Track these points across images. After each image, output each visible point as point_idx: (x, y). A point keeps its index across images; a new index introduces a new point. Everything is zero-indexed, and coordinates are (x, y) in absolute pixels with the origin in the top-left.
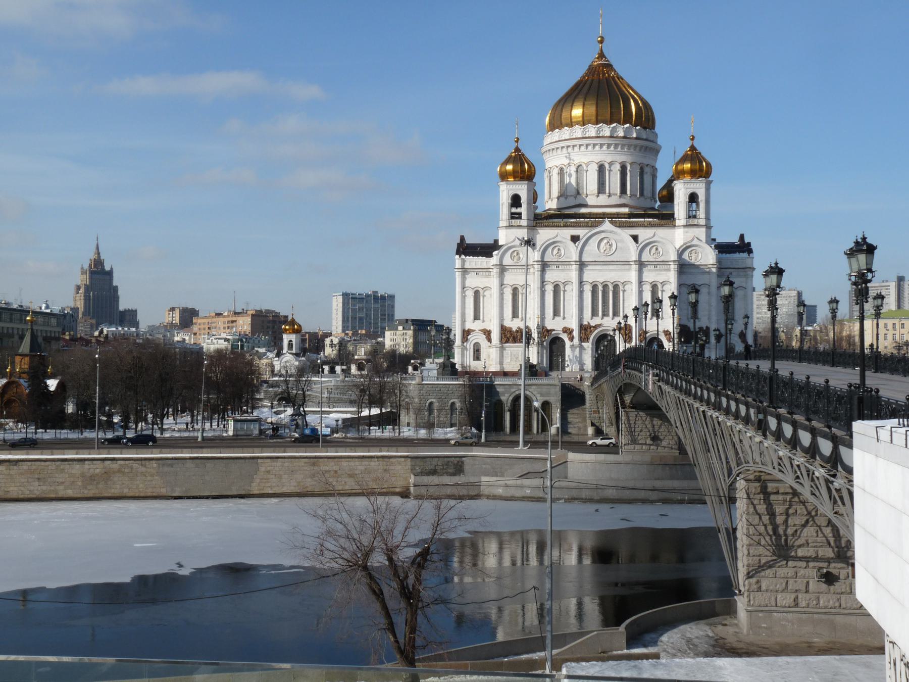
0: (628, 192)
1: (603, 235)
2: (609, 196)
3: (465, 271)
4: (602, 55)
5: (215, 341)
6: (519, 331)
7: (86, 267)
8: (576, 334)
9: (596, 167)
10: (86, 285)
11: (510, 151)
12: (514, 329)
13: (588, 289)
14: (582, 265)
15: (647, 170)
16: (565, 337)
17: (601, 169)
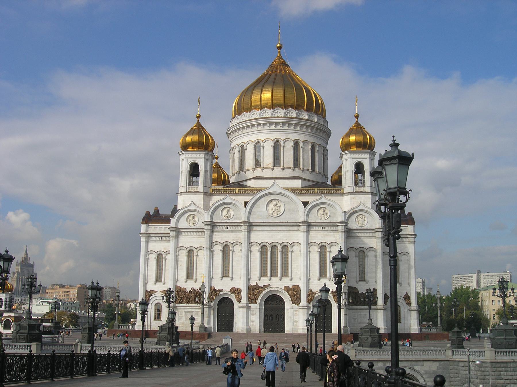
0: (301, 167)
1: (272, 197)
2: (283, 169)
3: (148, 235)
4: (280, 58)
5: (41, 303)
6: (193, 291)
7: (19, 262)
8: (244, 295)
9: (272, 143)
10: (18, 272)
11: (193, 124)
12: (188, 291)
13: (256, 250)
14: (250, 225)
15: (317, 149)
16: (233, 297)
17: (277, 145)
